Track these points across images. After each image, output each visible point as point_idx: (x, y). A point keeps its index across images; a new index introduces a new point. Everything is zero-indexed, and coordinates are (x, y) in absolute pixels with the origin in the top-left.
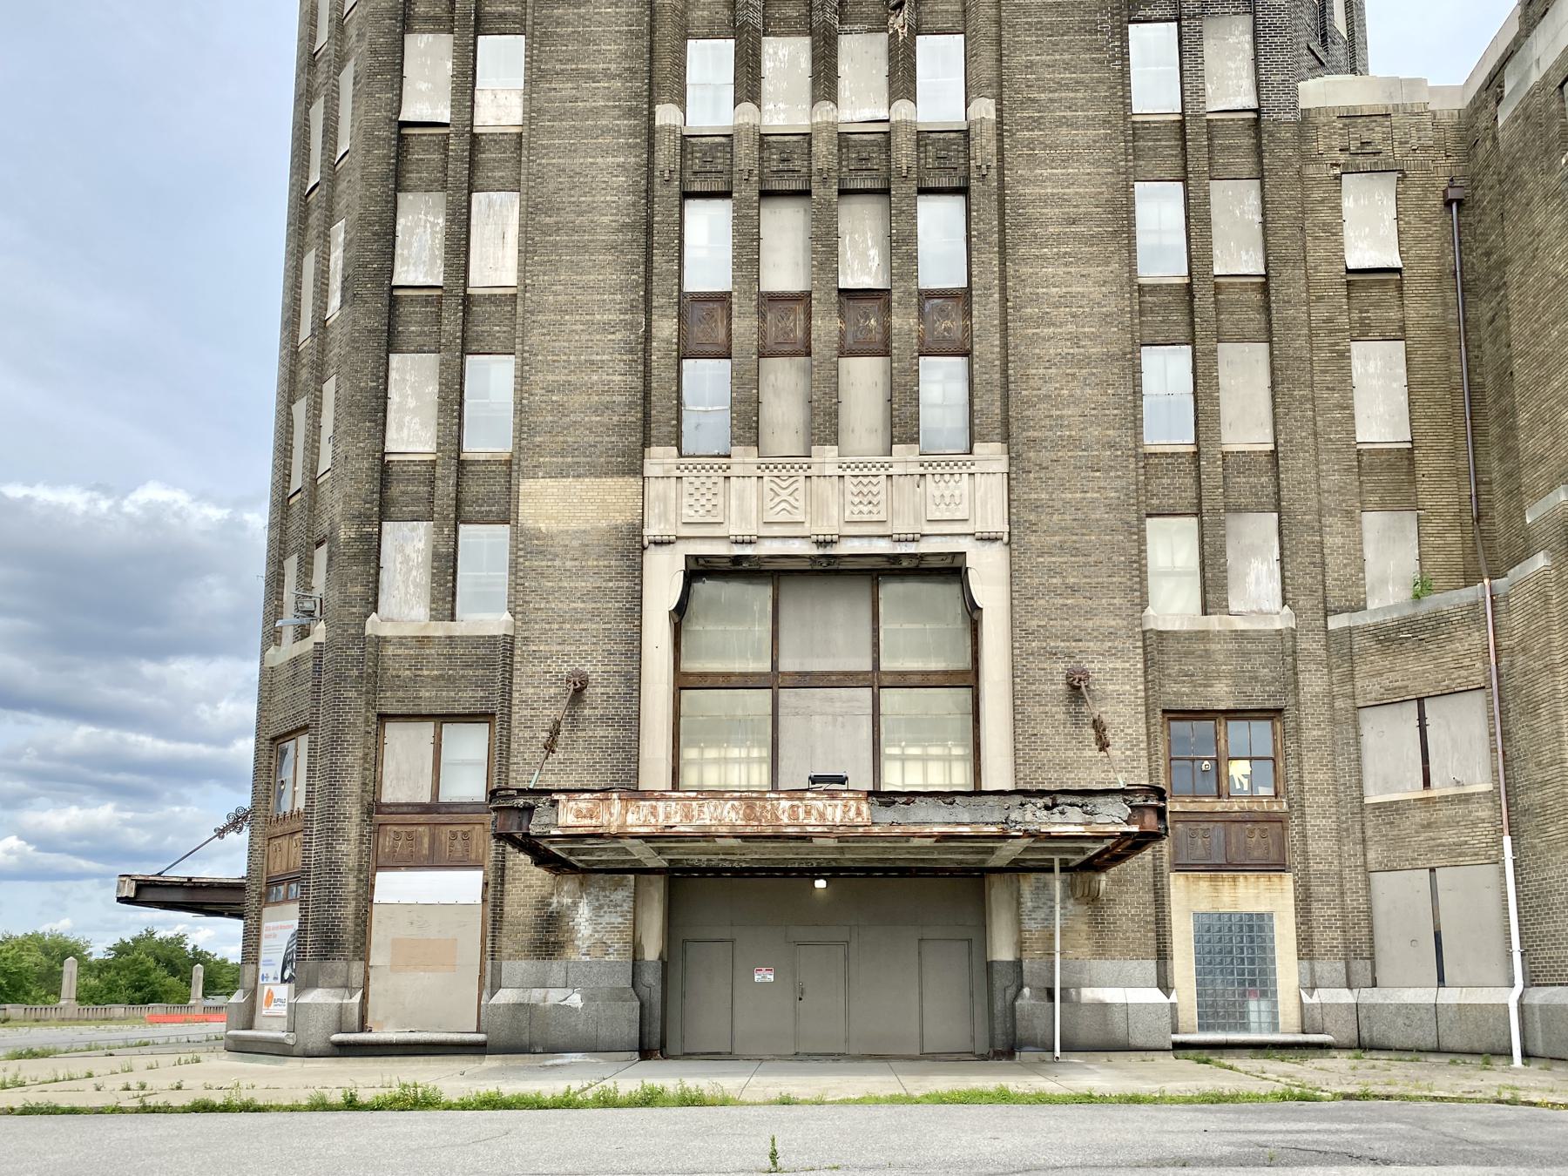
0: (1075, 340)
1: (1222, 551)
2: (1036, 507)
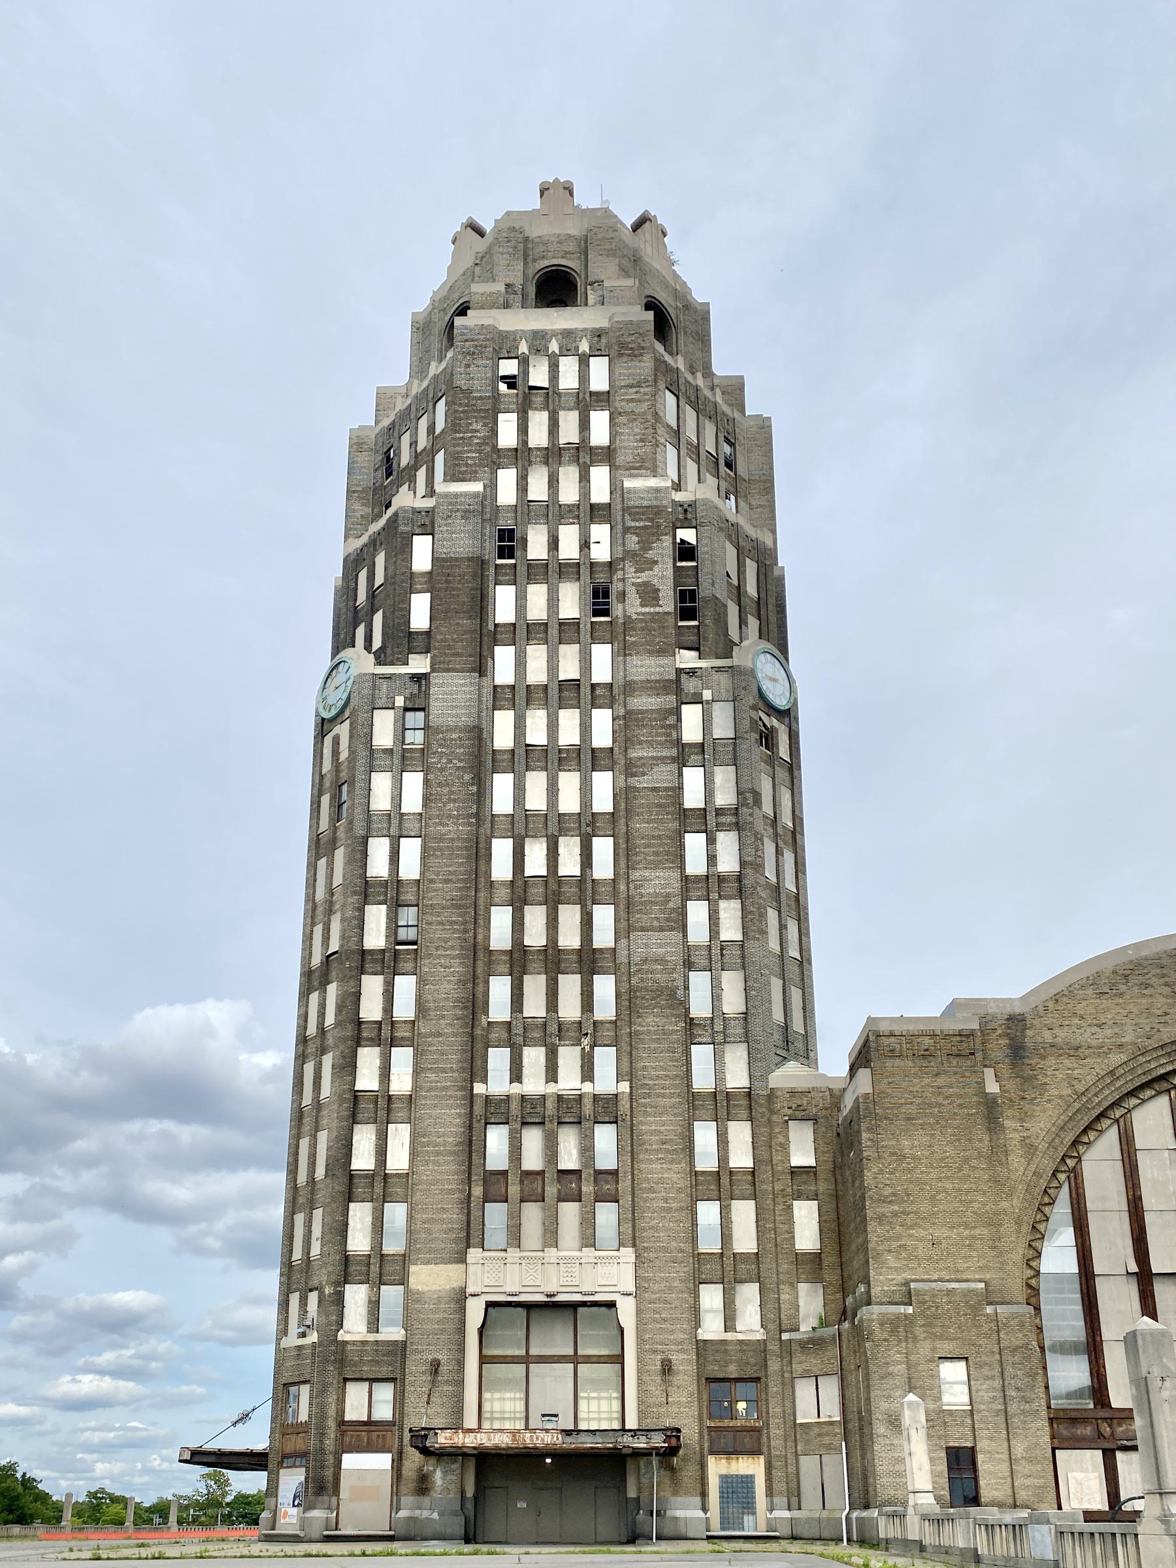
0: (666, 1200)
1: (733, 1301)
2: (648, 1280)
